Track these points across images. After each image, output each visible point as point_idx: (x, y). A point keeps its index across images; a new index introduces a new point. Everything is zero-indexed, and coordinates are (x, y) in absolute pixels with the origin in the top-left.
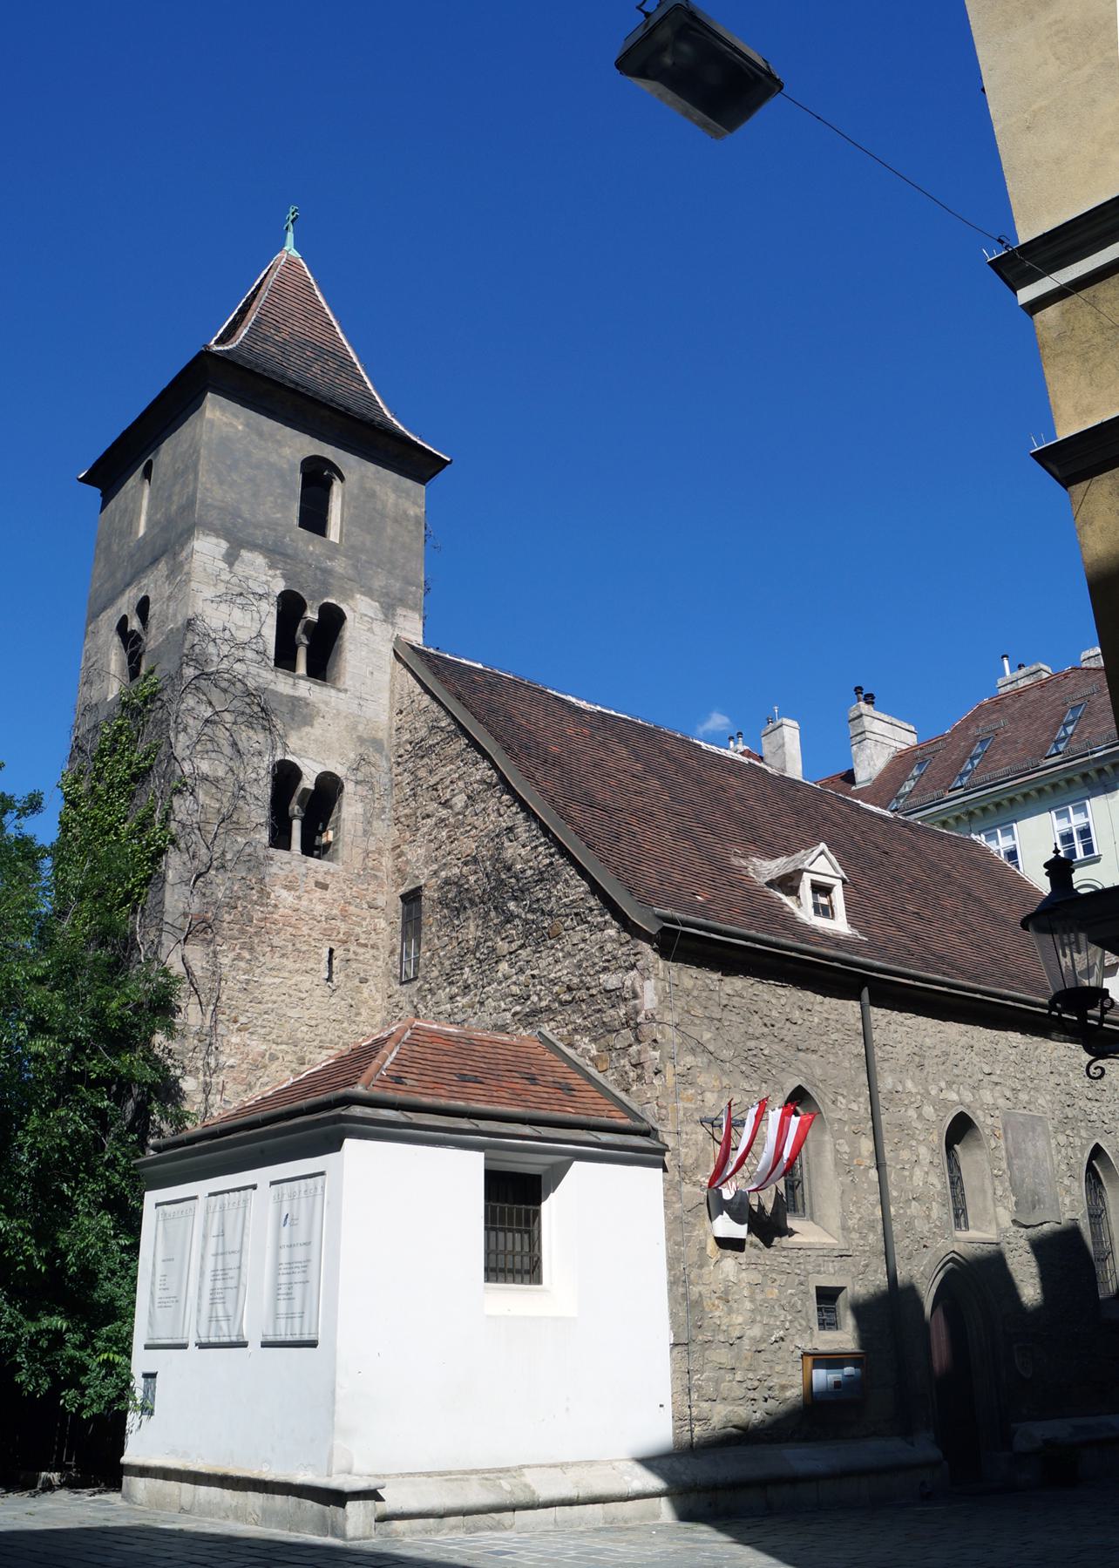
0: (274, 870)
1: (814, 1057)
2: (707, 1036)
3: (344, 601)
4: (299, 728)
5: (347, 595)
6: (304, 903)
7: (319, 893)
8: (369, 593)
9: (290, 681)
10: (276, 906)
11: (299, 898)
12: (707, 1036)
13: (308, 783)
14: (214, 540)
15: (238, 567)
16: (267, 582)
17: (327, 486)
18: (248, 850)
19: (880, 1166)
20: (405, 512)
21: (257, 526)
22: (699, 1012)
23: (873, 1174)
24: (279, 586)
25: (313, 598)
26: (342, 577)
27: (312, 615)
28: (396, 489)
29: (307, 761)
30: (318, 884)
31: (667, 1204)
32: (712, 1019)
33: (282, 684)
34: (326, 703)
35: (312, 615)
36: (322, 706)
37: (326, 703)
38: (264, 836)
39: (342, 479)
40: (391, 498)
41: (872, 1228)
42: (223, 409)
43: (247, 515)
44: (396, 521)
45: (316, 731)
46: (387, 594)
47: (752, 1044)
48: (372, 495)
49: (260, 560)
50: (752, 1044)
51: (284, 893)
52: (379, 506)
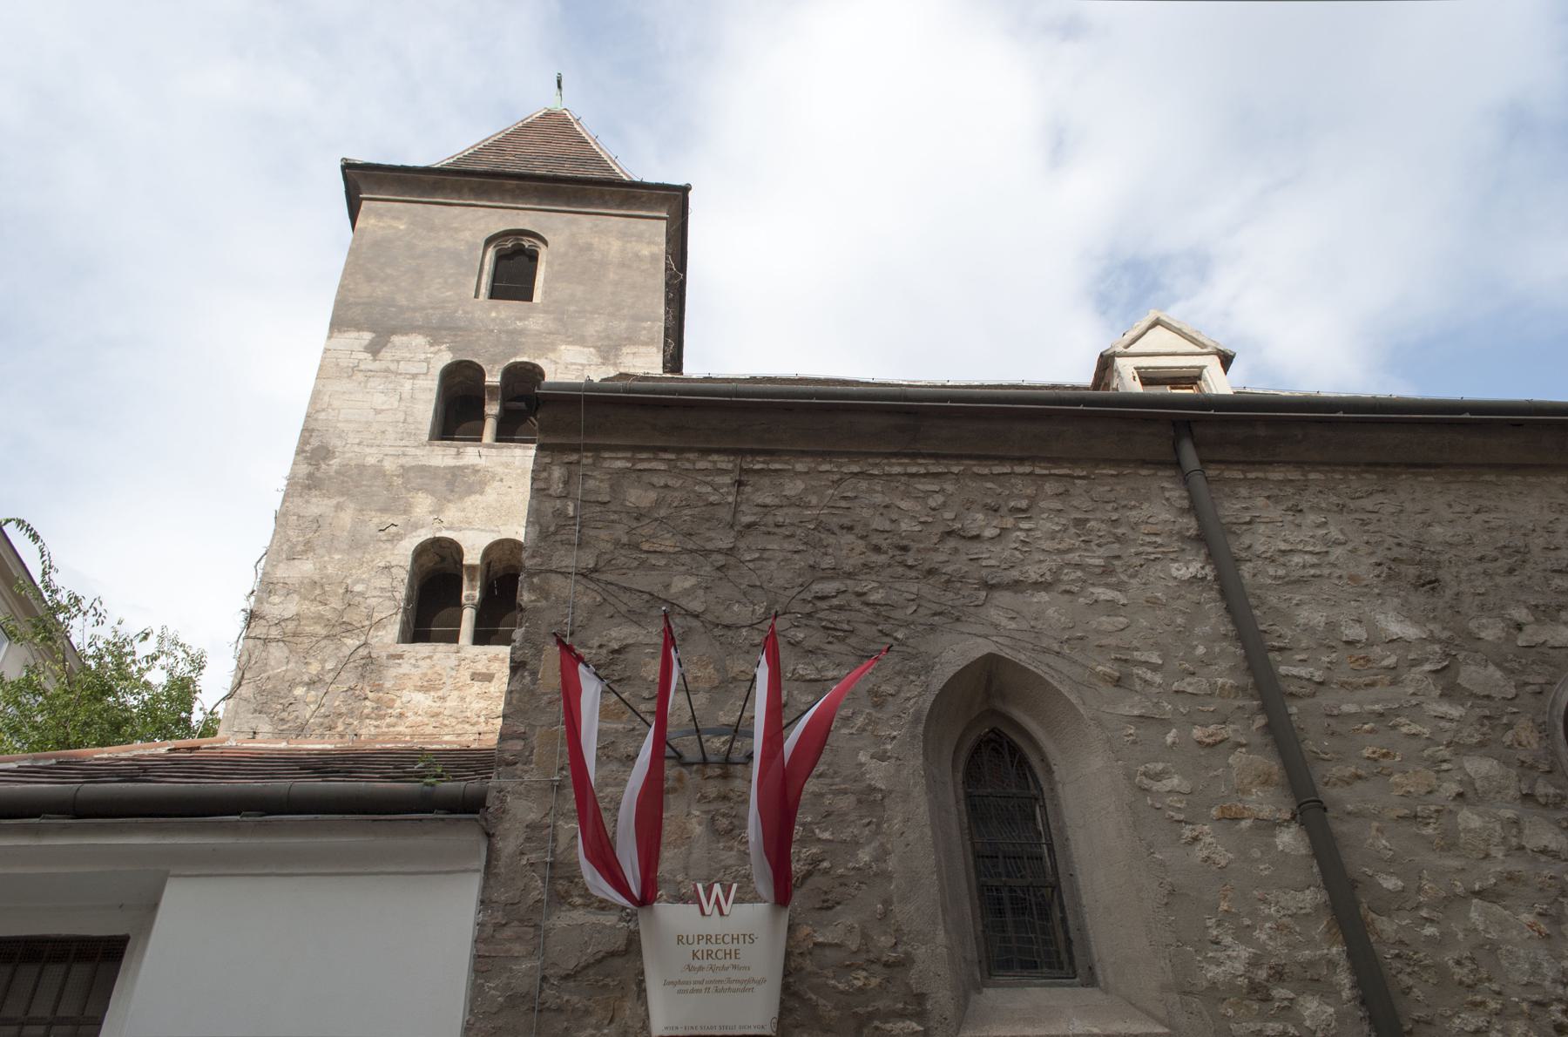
0: (405, 668)
1: (1043, 597)
2: (681, 583)
3: (539, 357)
4: (461, 498)
5: (547, 348)
6: (452, 702)
7: (477, 687)
8: (581, 341)
9: (453, 451)
10: (401, 715)
11: (443, 699)
12: (681, 583)
13: (472, 557)
14: (354, 334)
15: (386, 354)
16: (427, 360)
17: (533, 257)
18: (363, 652)
19: (1310, 810)
20: (637, 256)
21: (414, 310)
22: (668, 542)
23: (1289, 839)
24: (446, 358)
25: (493, 362)
26: (539, 334)
27: (493, 378)
28: (623, 235)
29: (469, 533)
30: (475, 677)
31: (484, 964)
32: (707, 553)
33: (444, 456)
34: (507, 465)
35: (493, 378)
36: (500, 470)
37: (507, 465)
38: (394, 630)
39: (545, 242)
40: (616, 245)
41: (1315, 983)
42: (380, 216)
43: (405, 303)
44: (622, 265)
45: (491, 494)
46: (608, 337)
47: (829, 587)
48: (589, 247)
49: (418, 340)
50: (829, 587)
51: (419, 697)
52: (597, 256)
